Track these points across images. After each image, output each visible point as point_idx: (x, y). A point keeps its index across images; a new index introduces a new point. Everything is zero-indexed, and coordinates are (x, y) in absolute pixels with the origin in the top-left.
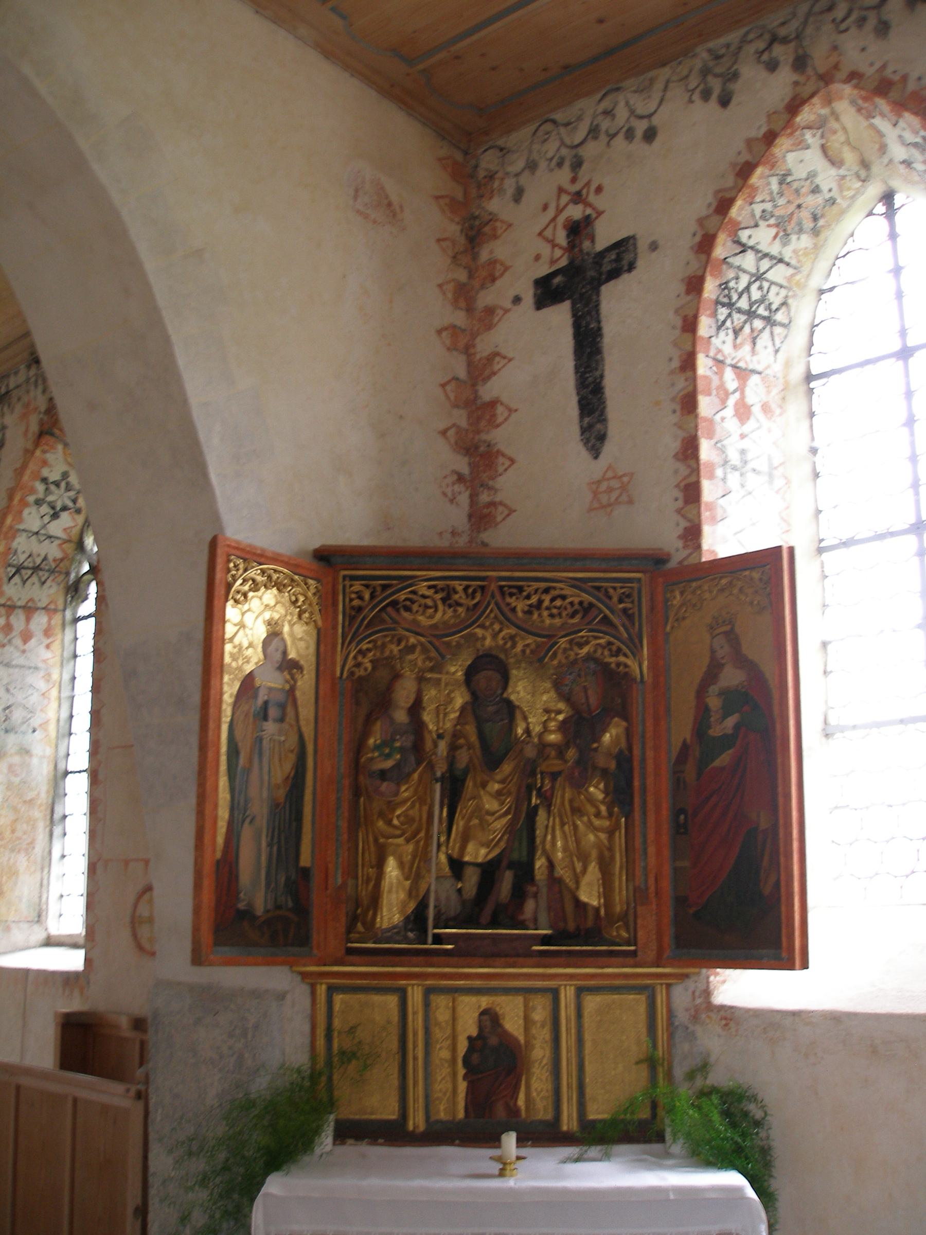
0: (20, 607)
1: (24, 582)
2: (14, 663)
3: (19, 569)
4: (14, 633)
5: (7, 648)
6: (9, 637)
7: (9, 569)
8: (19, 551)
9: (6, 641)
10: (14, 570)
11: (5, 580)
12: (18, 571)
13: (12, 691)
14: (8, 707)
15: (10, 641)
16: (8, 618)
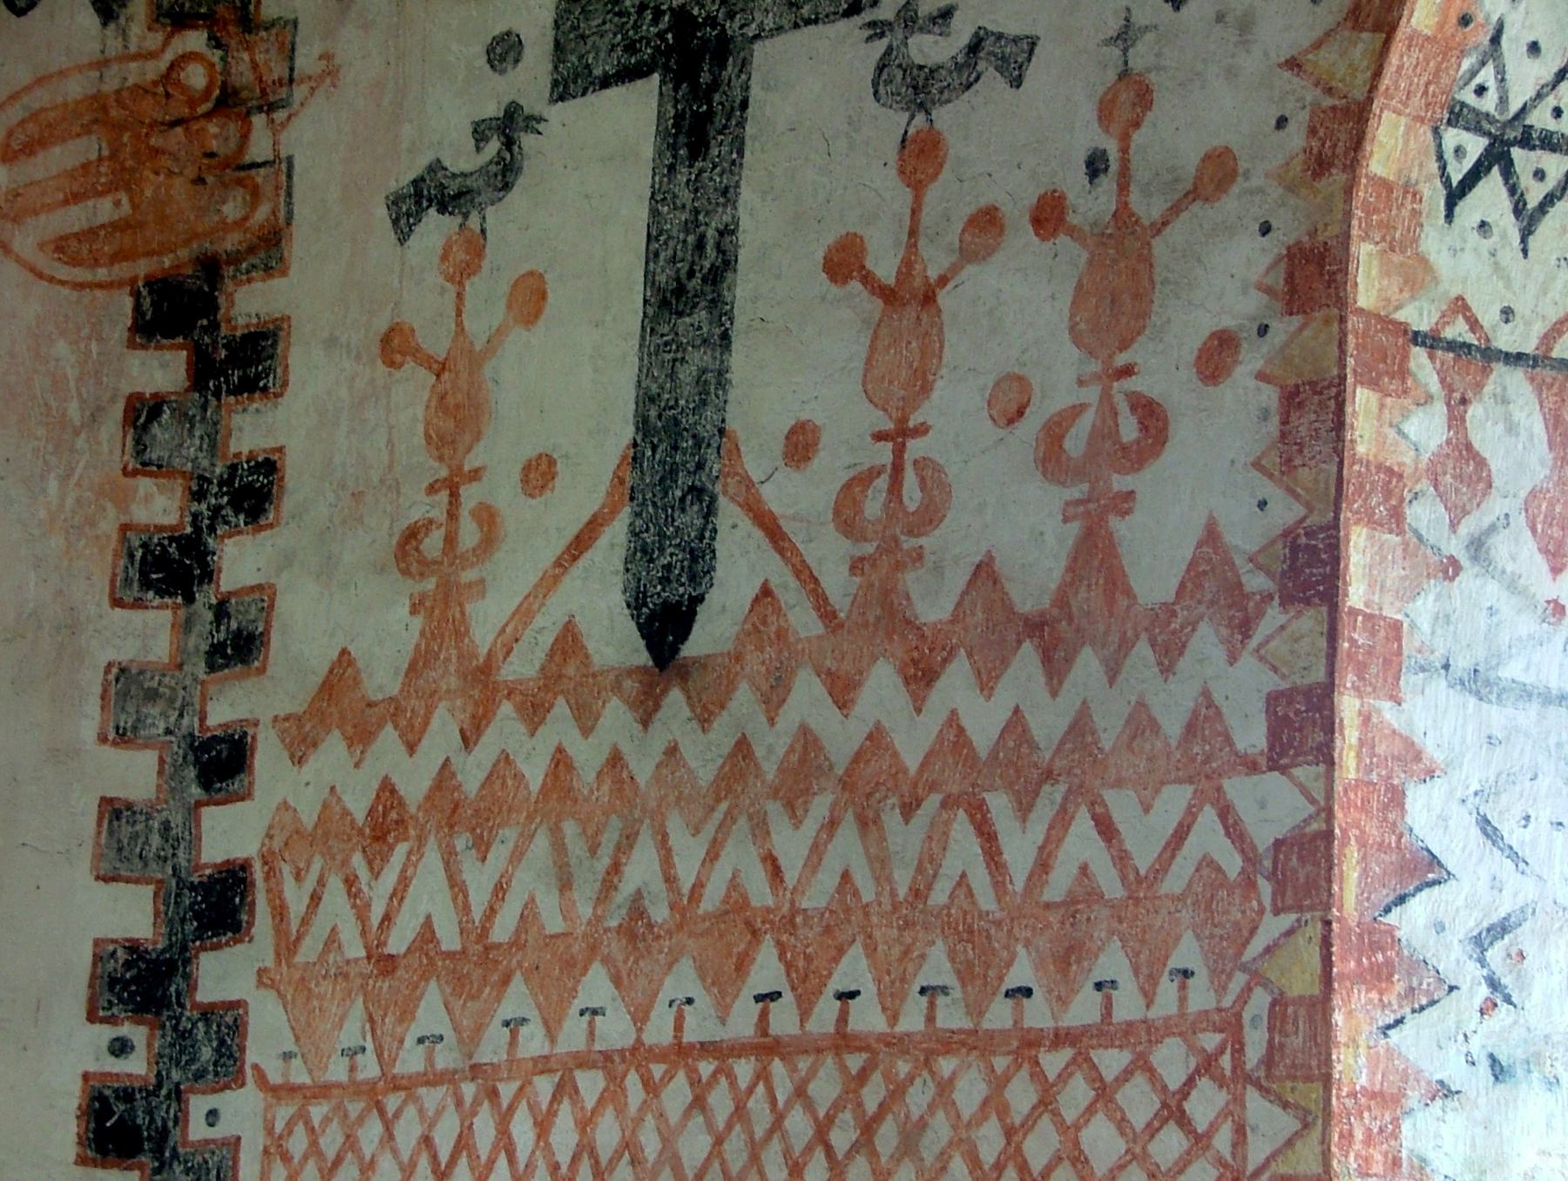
0: (1516, 359)
1: (1529, 219)
2: (1512, 671)
3: (1505, 144)
4: (1495, 507)
5: (1468, 579)
6: (1468, 527)
7: (1453, 137)
8: (1512, 47)
9: (1455, 546)
10: (1475, 146)
11: (1434, 195)
12: (1497, 157)
13: (1512, 833)
14: (1501, 929)
15: (1477, 546)
16: (1456, 419)
